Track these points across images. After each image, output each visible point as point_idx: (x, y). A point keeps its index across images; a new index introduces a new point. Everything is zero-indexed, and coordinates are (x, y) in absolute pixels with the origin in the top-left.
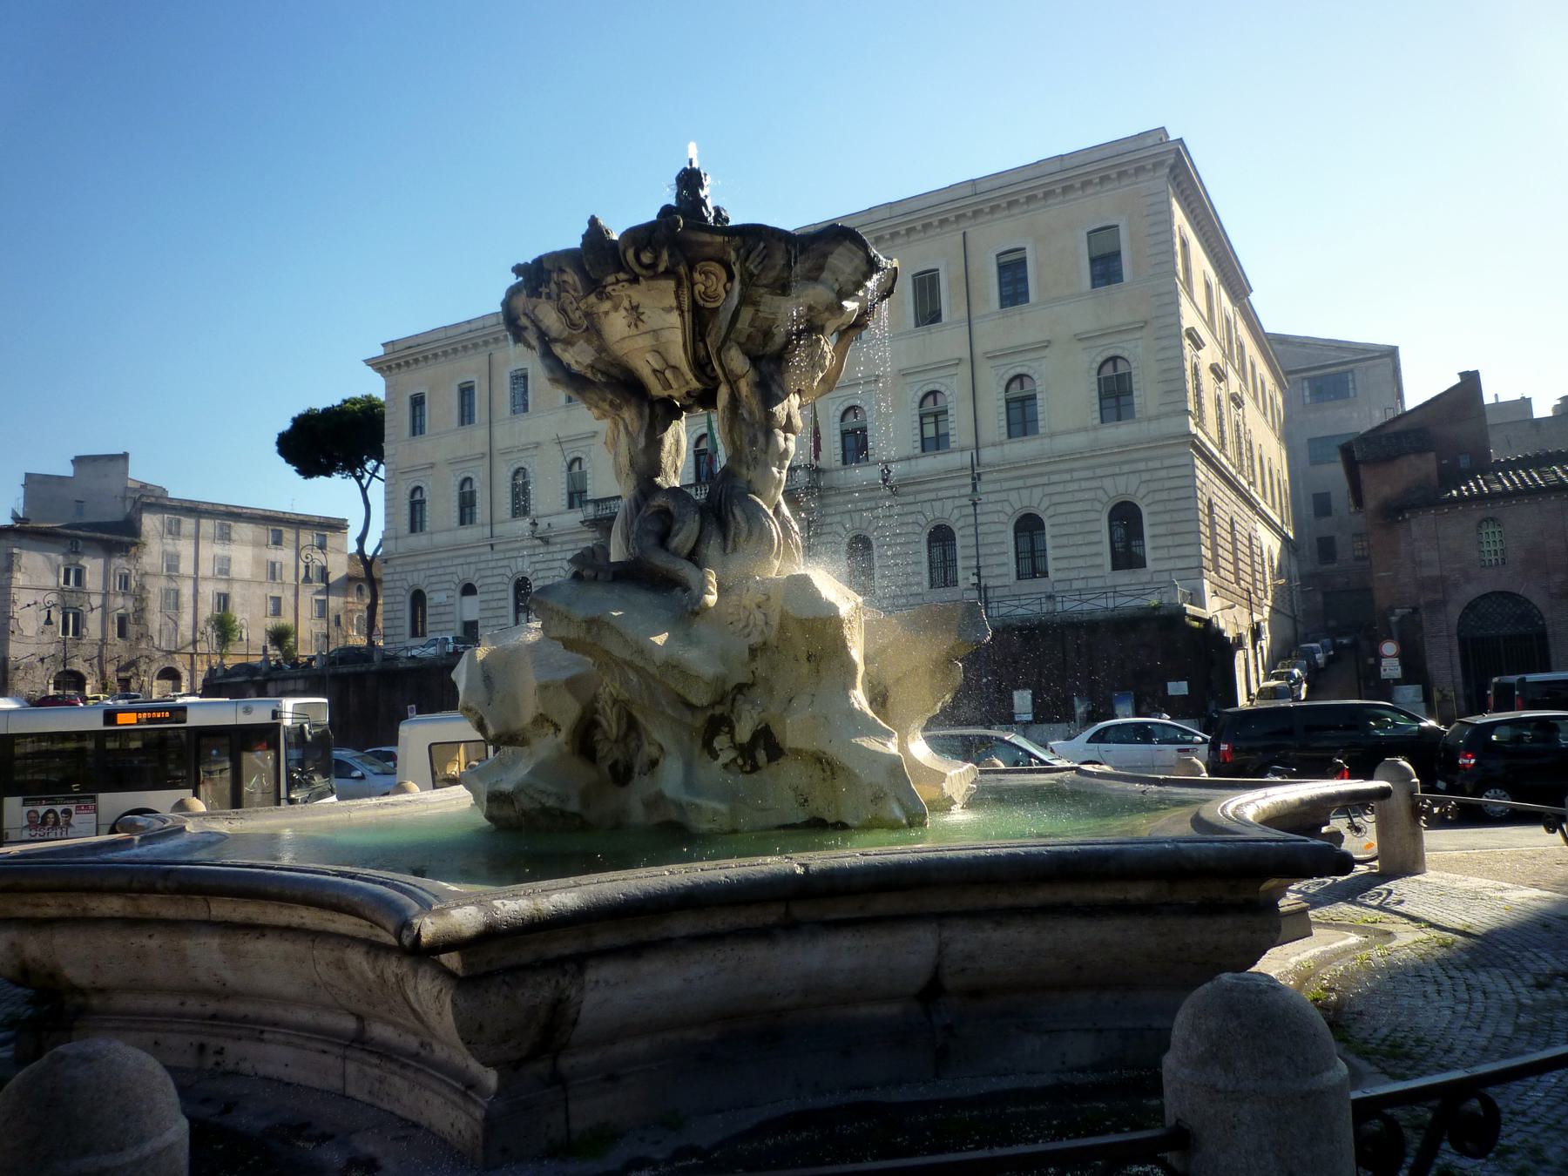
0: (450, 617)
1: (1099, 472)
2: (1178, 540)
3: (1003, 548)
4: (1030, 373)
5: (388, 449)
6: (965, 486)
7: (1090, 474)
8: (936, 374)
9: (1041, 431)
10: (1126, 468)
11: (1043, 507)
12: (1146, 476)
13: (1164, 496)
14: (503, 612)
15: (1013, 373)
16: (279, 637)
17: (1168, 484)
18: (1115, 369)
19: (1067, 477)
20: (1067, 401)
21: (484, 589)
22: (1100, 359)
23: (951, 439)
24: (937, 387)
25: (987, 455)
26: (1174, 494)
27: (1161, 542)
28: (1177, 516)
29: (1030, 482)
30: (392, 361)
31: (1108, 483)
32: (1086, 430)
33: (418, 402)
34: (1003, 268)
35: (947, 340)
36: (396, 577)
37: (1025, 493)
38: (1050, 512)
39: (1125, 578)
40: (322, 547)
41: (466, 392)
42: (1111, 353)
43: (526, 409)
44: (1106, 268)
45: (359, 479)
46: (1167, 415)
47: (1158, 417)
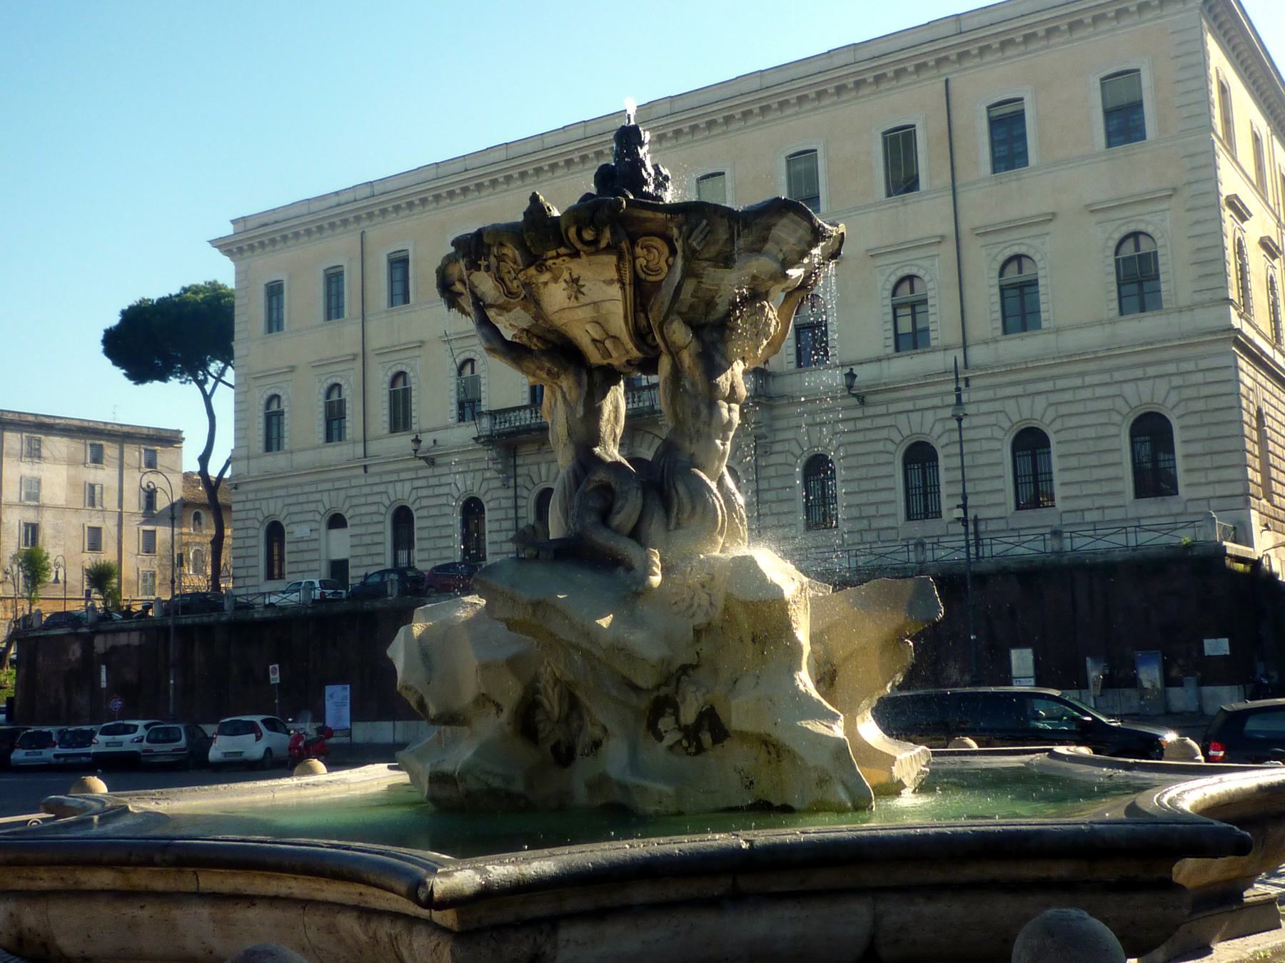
0: (315, 556)
1: (1118, 376)
2: (1219, 460)
3: (998, 471)
4: (1030, 253)
5: (238, 348)
6: (949, 393)
7: (1105, 378)
8: (913, 254)
9: (1044, 324)
10: (1151, 371)
11: (1047, 420)
12: (1177, 381)
13: (1200, 405)
14: (379, 549)
15: (1009, 253)
16: (100, 577)
17: (1206, 391)
18: (1137, 248)
19: (1078, 382)
20: (1077, 290)
21: (356, 521)
22: (1117, 236)
23: (932, 335)
24: (913, 271)
25: (978, 355)
26: (1214, 403)
27: (1196, 463)
28: (1216, 431)
29: (1032, 388)
30: (245, 241)
31: (1128, 389)
32: (1101, 323)
33: (274, 291)
34: (994, 123)
35: (925, 213)
36: (249, 505)
37: (1025, 403)
38: (1057, 425)
39: (1152, 508)
40: (151, 464)
41: (334, 279)
42: (1132, 228)
43: (406, 300)
45: (201, 384)
46: (1202, 305)
47: (1191, 308)
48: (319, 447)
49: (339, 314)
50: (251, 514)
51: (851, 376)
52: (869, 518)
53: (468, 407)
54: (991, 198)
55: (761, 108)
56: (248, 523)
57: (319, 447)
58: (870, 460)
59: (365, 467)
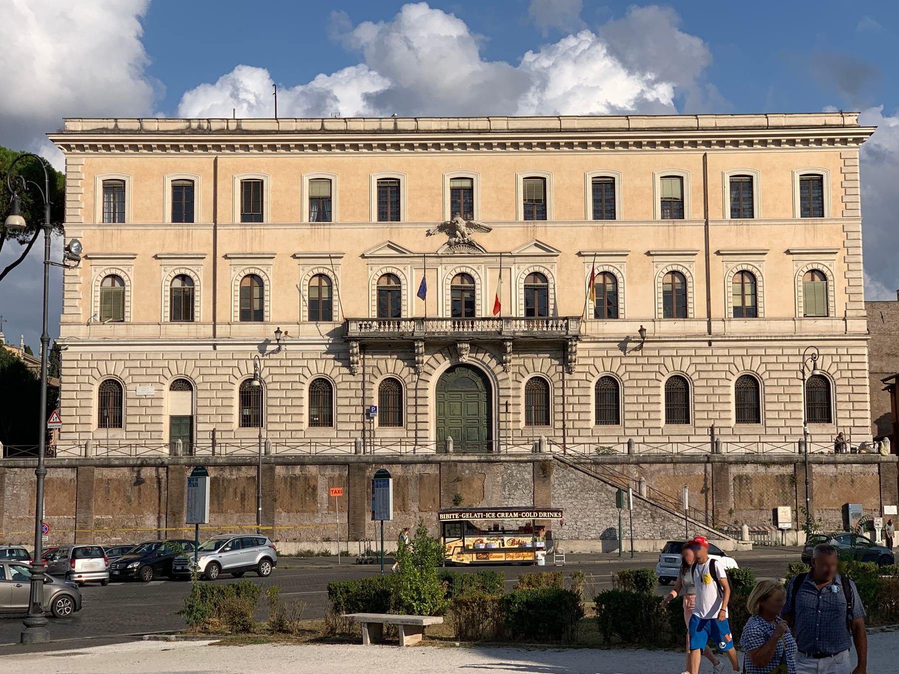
12: (837, 359)
46: (853, 318)
48: (165, 323)
49: (190, 218)
50: (89, 372)
51: (642, 330)
52: (644, 420)
53: (320, 309)
54: (729, 234)
56: (81, 379)
57: (165, 323)
59: (215, 346)
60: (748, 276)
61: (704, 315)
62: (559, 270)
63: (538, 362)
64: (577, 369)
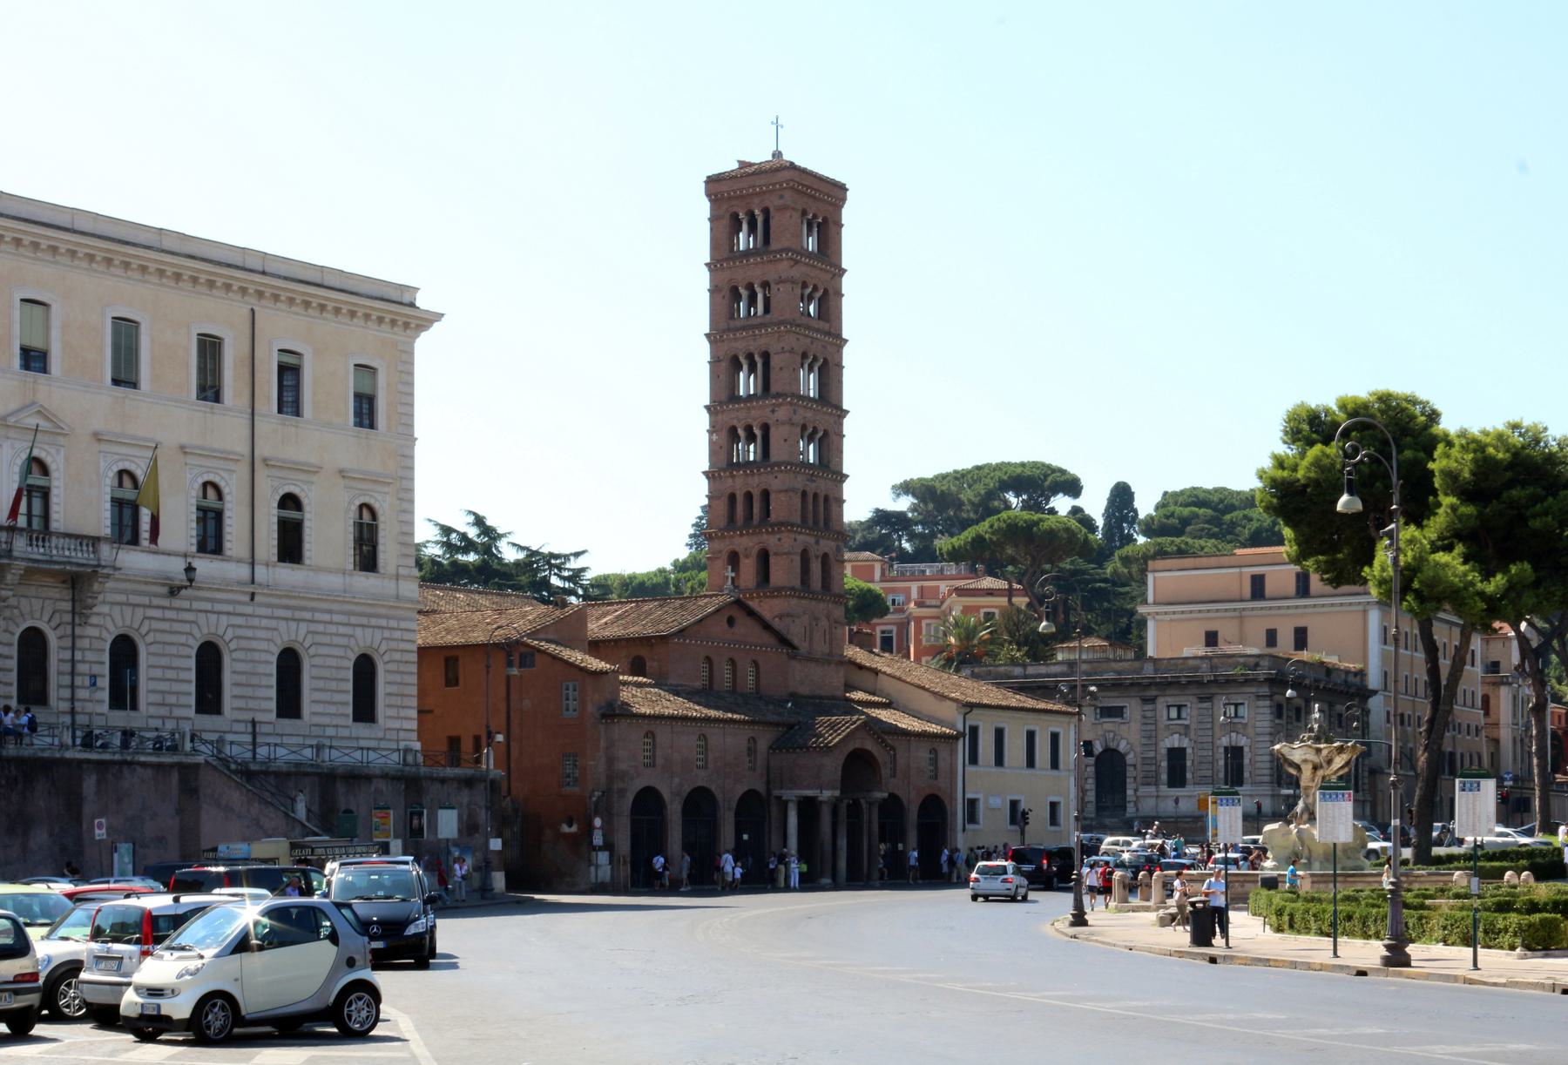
1: (353, 620)
9: (307, 561)
12: (387, 634)
44: (365, 411)
52: (171, 705)
55: (87, 254)
58: (173, 650)
60: (290, 501)
61: (245, 553)
62: (67, 459)
63: (37, 604)
64: (94, 620)
